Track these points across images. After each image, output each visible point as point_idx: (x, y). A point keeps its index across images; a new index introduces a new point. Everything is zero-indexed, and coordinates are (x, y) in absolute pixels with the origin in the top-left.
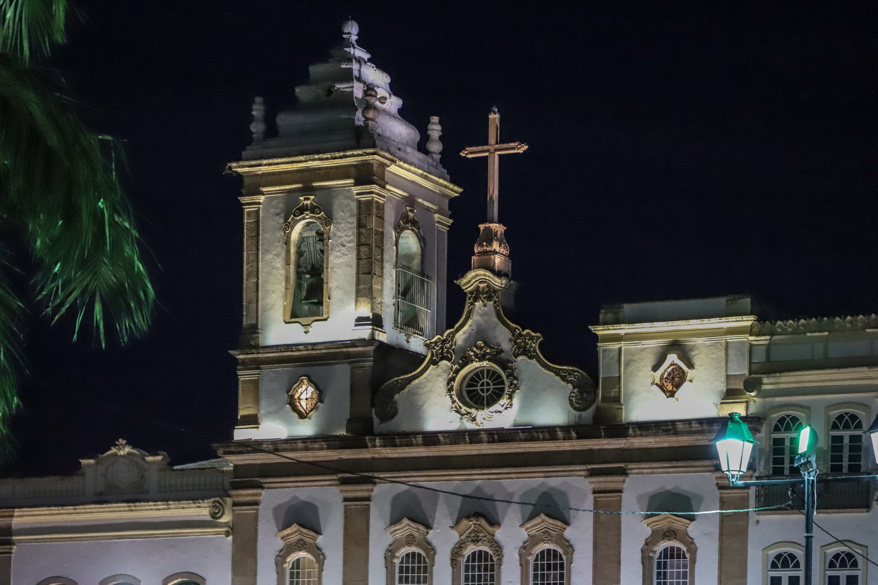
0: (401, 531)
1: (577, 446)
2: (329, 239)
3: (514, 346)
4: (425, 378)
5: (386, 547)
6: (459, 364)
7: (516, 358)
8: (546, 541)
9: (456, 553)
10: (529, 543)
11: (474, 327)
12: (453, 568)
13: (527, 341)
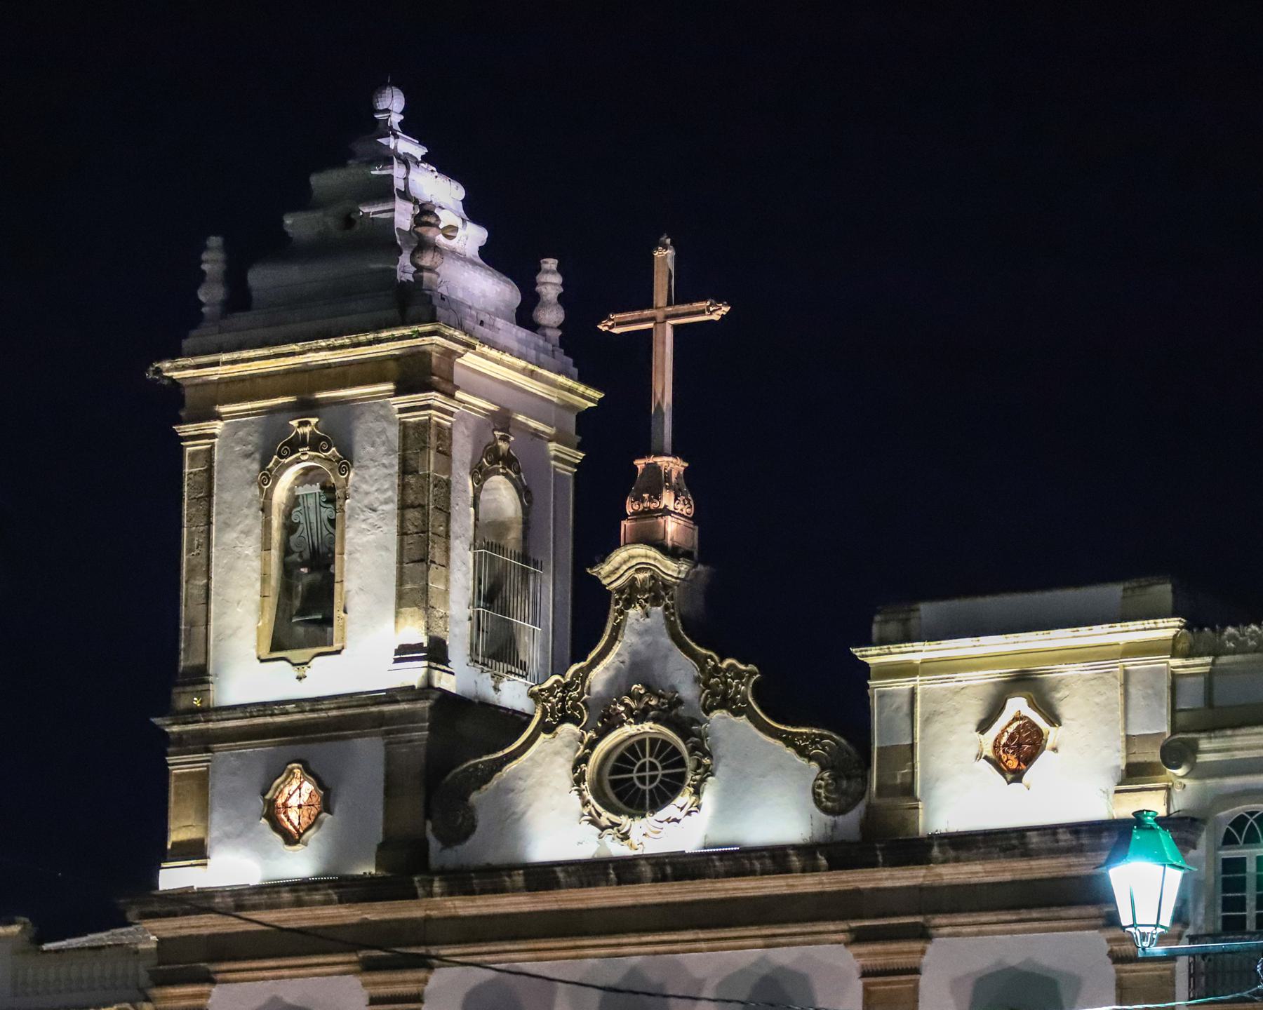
6: (596, 730)
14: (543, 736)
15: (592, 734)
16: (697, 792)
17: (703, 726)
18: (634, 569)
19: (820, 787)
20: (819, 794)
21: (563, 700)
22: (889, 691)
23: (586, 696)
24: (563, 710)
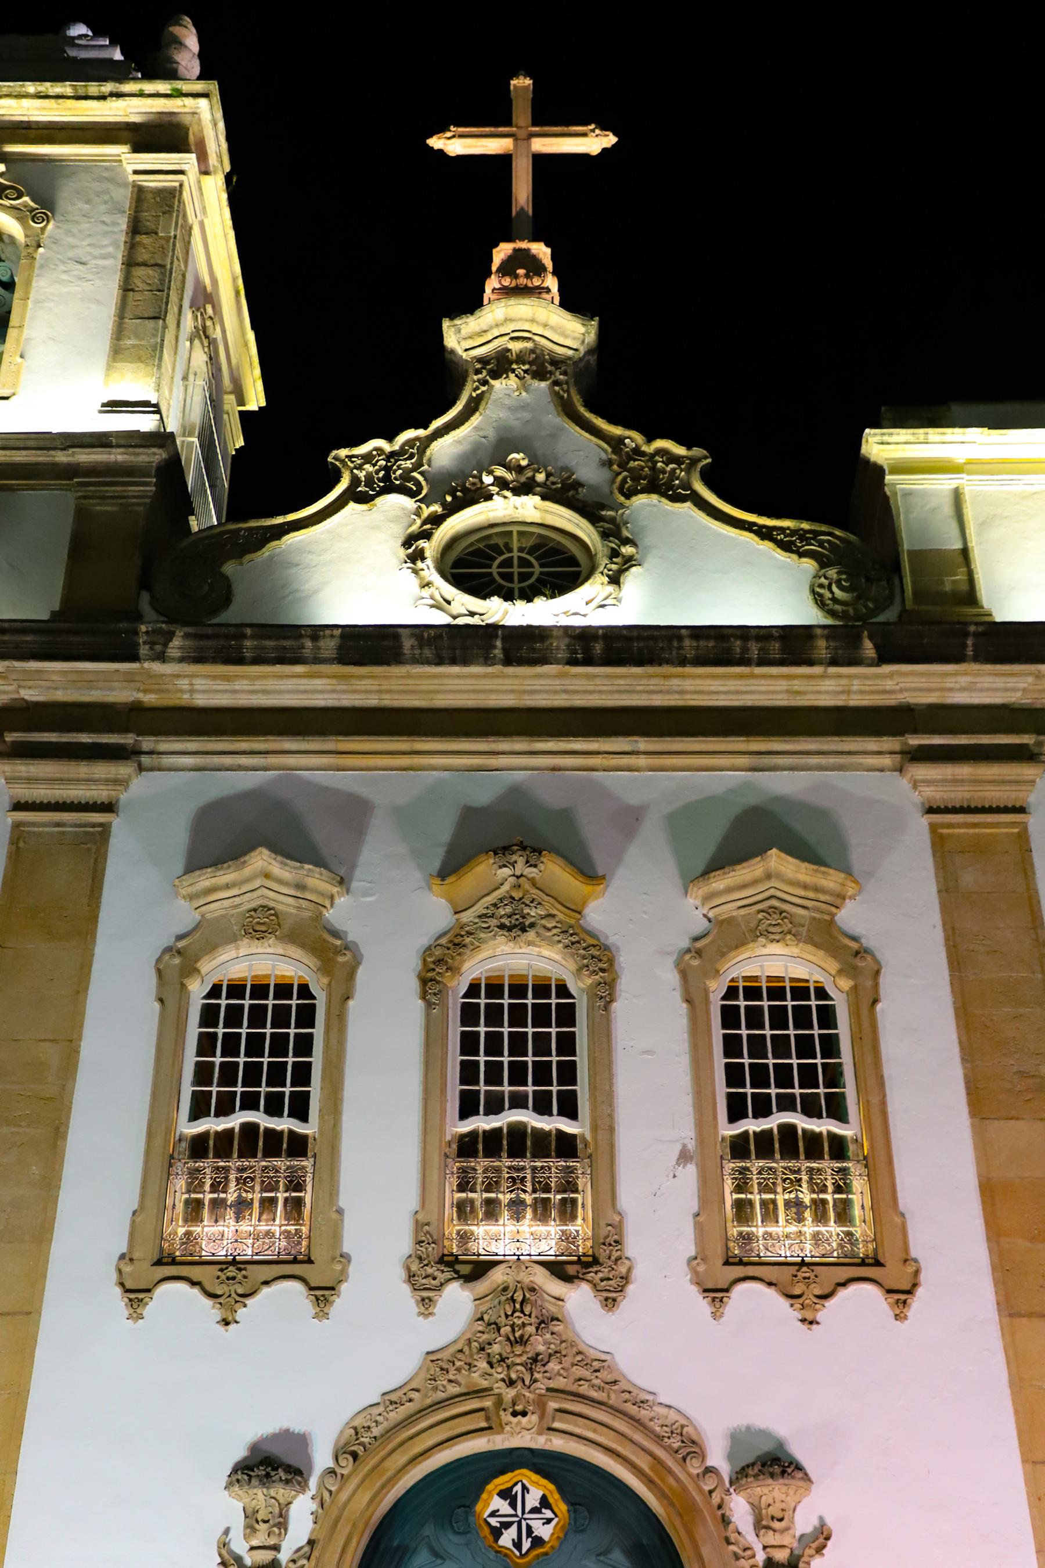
0: (235, 891)
1: (861, 692)
2: (39, 246)
3: (619, 474)
4: (329, 532)
5: (167, 941)
6: (444, 505)
7: (628, 497)
9: (439, 961)
11: (491, 433)
13: (659, 464)
14: (352, 506)
15: (436, 508)
16: (615, 580)
17: (620, 512)
18: (509, 337)
19: (821, 586)
20: (821, 595)
21: (387, 469)
22: (919, 490)
23: (426, 467)
24: (387, 478)
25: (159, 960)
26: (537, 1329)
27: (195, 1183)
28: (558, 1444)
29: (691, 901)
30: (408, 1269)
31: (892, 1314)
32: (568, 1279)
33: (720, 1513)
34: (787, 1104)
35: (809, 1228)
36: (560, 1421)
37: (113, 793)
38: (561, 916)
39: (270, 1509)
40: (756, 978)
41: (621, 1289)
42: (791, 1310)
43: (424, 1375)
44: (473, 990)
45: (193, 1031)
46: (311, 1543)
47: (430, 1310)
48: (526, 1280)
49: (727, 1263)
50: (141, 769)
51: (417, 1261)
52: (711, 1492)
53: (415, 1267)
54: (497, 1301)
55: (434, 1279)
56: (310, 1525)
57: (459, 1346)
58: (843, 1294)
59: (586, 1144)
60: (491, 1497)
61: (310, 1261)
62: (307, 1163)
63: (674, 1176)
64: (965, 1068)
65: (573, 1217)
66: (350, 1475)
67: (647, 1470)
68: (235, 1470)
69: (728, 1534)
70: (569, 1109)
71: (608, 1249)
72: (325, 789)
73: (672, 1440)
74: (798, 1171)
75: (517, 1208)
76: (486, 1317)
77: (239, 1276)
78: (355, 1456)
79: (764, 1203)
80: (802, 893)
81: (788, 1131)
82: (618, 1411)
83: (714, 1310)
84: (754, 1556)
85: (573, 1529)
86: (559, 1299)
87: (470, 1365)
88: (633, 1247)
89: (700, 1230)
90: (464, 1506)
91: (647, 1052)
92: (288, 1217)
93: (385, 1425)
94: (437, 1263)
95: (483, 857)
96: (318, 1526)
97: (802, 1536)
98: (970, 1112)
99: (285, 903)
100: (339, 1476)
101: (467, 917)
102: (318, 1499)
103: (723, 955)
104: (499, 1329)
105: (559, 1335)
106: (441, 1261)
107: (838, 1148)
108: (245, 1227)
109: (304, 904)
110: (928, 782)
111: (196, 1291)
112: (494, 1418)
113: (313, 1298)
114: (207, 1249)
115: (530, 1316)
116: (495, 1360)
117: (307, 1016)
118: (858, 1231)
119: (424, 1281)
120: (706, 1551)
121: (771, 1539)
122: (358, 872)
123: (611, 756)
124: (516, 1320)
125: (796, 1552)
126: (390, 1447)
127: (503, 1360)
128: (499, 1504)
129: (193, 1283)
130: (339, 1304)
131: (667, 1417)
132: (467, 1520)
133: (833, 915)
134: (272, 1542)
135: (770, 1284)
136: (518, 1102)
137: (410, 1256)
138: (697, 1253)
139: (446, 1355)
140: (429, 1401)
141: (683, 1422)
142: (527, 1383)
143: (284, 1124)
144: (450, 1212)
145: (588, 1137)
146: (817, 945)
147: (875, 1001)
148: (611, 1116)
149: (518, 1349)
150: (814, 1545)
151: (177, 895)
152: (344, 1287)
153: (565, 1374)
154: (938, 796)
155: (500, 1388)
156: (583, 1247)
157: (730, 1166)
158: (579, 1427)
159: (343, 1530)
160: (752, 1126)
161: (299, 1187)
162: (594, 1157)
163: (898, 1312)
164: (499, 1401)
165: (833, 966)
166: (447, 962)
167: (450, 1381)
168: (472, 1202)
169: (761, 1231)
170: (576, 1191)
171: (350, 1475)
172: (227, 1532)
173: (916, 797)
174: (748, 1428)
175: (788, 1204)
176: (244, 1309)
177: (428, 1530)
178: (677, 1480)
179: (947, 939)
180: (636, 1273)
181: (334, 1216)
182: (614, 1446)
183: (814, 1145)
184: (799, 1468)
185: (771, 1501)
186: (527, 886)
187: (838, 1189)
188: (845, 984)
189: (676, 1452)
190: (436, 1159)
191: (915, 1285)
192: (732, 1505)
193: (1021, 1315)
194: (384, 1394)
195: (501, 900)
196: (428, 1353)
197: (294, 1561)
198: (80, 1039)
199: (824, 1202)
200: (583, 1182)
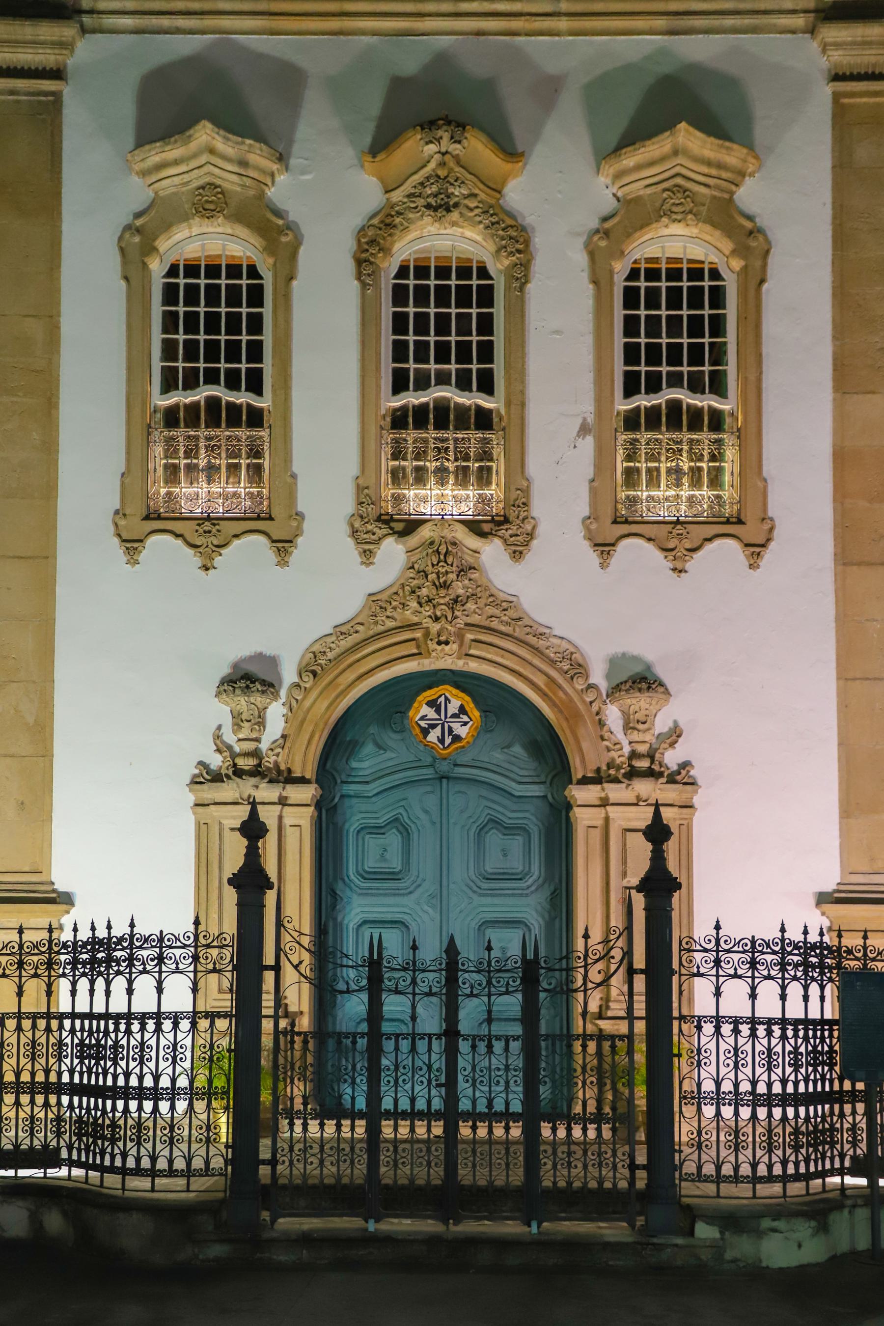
0: (183, 168)
5: (125, 218)
8: (679, 217)
10: (619, 223)
12: (364, 286)
25: (120, 238)
26: (458, 576)
27: (171, 450)
28: (474, 666)
29: (602, 180)
30: (352, 526)
31: (747, 564)
32: (482, 535)
33: (597, 718)
34: (675, 380)
35: (685, 493)
36: (475, 648)
37: (60, 58)
38: (482, 196)
39: (251, 712)
40: (656, 260)
41: (527, 544)
42: (665, 561)
43: (367, 612)
44: (403, 272)
45: (157, 309)
46: (284, 737)
47: (371, 560)
48: (449, 535)
49: (615, 522)
50: (84, 31)
51: (360, 519)
52: (591, 703)
53: (357, 525)
54: (425, 553)
55: (374, 534)
56: (282, 724)
57: (394, 590)
58: (709, 547)
59: (501, 418)
60: (420, 706)
61: (271, 518)
62: (264, 433)
63: (575, 447)
64: (834, 346)
65: (489, 483)
66: (311, 688)
67: (543, 687)
68: (222, 683)
69: (603, 733)
70: (487, 385)
71: (517, 510)
72: (261, 56)
73: (563, 664)
74: (680, 442)
75: (441, 474)
76: (416, 566)
77: (214, 530)
78: (314, 673)
79: (649, 471)
80: (705, 170)
81: (675, 407)
82: (521, 641)
83: (602, 561)
84: (621, 749)
85: (485, 729)
86: (475, 552)
87: (403, 604)
88: (537, 509)
89: (594, 493)
90: (401, 712)
91: (557, 332)
92: (250, 480)
93: (337, 651)
94: (376, 521)
95: (410, 133)
96: (288, 725)
97: (659, 734)
98: (834, 387)
99: (231, 181)
100: (303, 689)
101: (397, 196)
102: (288, 705)
103: (629, 235)
104: (427, 577)
105: (476, 581)
106: (379, 519)
107: (716, 421)
108: (216, 489)
109: (248, 182)
110: (838, 45)
111: (179, 542)
112: (423, 646)
113: (275, 549)
114: (185, 508)
115: (452, 565)
116: (423, 601)
117: (256, 296)
118: (726, 495)
119: (365, 536)
120: (585, 745)
121: (636, 736)
122: (296, 149)
123: (534, 18)
124: (440, 569)
125: (654, 746)
126: (342, 667)
127: (430, 601)
128: (426, 710)
129: (177, 536)
130: (297, 555)
131: (559, 646)
132: (402, 722)
133: (732, 193)
134: (254, 735)
135: (650, 540)
136: (443, 379)
137: (353, 515)
138: (591, 513)
139: (384, 596)
140: (371, 633)
141: (573, 650)
142: (449, 619)
143: (243, 398)
144: (385, 477)
145: (503, 412)
146: (714, 225)
147: (762, 281)
148: (523, 392)
149: (442, 592)
150: (668, 741)
151: (130, 169)
152: (300, 540)
153: (480, 612)
154: (845, 60)
155: (428, 623)
156: (496, 508)
157: (622, 437)
158: (489, 653)
159: (308, 728)
160: (643, 401)
161: (258, 454)
162: (507, 430)
163: (752, 562)
164: (427, 634)
165: (727, 246)
166: (379, 244)
167: (388, 617)
168: (404, 469)
169: (645, 494)
170: (491, 460)
171: (311, 688)
172: (219, 727)
173: (824, 63)
174: (624, 654)
175: (669, 471)
176: (220, 558)
177: (373, 729)
178: (566, 694)
179: (834, 218)
180: (540, 530)
181: (289, 480)
182: (517, 668)
183: (696, 419)
184: (661, 684)
185: (637, 709)
186: (452, 164)
187: (713, 458)
188: (737, 264)
189: (566, 673)
190: (373, 430)
191: (769, 540)
192: (607, 712)
193: (853, 564)
194: (335, 627)
195: (428, 178)
196: (370, 595)
197: (272, 750)
198: (59, 316)
199: (700, 469)
200: (497, 452)
